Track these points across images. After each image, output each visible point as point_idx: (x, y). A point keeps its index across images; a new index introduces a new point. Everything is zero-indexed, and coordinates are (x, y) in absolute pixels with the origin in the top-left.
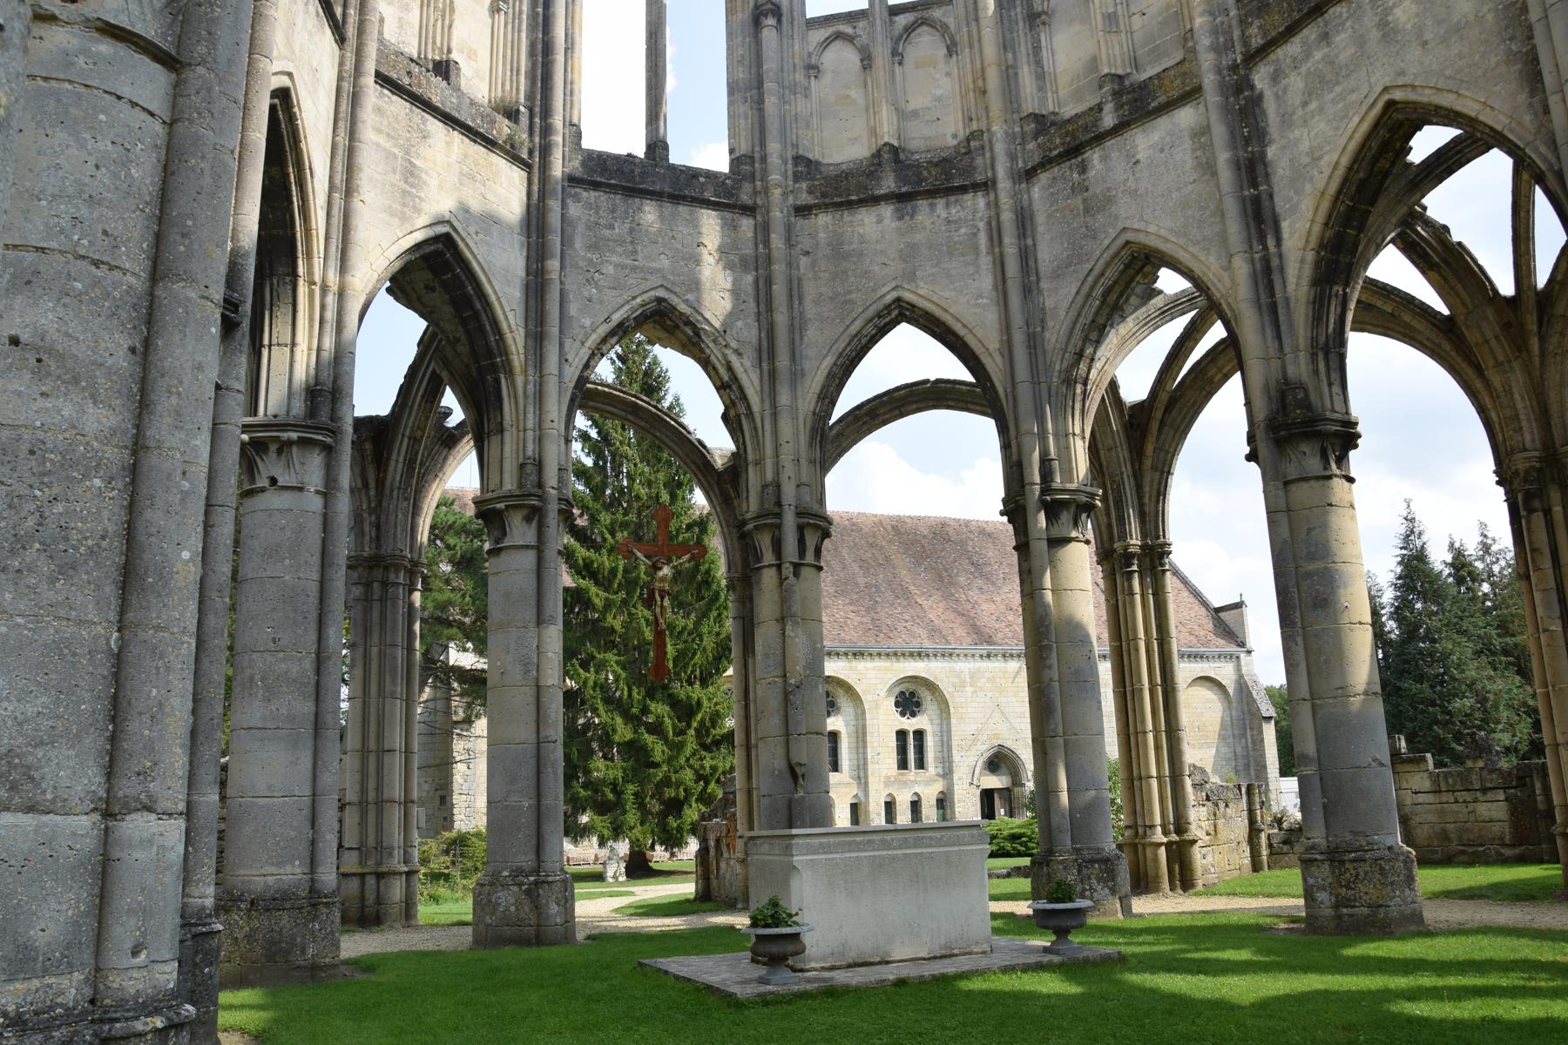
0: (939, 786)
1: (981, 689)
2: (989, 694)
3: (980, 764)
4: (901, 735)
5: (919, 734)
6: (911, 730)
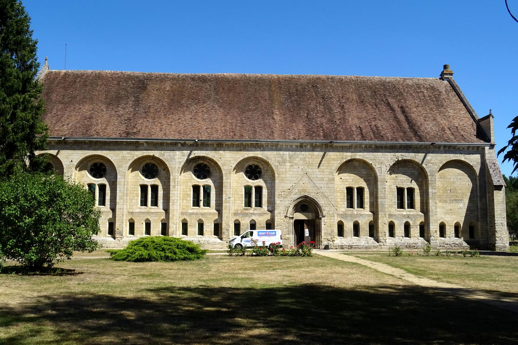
0: (268, 217)
1: (296, 164)
2: (301, 167)
3: (292, 206)
6: (97, 183)
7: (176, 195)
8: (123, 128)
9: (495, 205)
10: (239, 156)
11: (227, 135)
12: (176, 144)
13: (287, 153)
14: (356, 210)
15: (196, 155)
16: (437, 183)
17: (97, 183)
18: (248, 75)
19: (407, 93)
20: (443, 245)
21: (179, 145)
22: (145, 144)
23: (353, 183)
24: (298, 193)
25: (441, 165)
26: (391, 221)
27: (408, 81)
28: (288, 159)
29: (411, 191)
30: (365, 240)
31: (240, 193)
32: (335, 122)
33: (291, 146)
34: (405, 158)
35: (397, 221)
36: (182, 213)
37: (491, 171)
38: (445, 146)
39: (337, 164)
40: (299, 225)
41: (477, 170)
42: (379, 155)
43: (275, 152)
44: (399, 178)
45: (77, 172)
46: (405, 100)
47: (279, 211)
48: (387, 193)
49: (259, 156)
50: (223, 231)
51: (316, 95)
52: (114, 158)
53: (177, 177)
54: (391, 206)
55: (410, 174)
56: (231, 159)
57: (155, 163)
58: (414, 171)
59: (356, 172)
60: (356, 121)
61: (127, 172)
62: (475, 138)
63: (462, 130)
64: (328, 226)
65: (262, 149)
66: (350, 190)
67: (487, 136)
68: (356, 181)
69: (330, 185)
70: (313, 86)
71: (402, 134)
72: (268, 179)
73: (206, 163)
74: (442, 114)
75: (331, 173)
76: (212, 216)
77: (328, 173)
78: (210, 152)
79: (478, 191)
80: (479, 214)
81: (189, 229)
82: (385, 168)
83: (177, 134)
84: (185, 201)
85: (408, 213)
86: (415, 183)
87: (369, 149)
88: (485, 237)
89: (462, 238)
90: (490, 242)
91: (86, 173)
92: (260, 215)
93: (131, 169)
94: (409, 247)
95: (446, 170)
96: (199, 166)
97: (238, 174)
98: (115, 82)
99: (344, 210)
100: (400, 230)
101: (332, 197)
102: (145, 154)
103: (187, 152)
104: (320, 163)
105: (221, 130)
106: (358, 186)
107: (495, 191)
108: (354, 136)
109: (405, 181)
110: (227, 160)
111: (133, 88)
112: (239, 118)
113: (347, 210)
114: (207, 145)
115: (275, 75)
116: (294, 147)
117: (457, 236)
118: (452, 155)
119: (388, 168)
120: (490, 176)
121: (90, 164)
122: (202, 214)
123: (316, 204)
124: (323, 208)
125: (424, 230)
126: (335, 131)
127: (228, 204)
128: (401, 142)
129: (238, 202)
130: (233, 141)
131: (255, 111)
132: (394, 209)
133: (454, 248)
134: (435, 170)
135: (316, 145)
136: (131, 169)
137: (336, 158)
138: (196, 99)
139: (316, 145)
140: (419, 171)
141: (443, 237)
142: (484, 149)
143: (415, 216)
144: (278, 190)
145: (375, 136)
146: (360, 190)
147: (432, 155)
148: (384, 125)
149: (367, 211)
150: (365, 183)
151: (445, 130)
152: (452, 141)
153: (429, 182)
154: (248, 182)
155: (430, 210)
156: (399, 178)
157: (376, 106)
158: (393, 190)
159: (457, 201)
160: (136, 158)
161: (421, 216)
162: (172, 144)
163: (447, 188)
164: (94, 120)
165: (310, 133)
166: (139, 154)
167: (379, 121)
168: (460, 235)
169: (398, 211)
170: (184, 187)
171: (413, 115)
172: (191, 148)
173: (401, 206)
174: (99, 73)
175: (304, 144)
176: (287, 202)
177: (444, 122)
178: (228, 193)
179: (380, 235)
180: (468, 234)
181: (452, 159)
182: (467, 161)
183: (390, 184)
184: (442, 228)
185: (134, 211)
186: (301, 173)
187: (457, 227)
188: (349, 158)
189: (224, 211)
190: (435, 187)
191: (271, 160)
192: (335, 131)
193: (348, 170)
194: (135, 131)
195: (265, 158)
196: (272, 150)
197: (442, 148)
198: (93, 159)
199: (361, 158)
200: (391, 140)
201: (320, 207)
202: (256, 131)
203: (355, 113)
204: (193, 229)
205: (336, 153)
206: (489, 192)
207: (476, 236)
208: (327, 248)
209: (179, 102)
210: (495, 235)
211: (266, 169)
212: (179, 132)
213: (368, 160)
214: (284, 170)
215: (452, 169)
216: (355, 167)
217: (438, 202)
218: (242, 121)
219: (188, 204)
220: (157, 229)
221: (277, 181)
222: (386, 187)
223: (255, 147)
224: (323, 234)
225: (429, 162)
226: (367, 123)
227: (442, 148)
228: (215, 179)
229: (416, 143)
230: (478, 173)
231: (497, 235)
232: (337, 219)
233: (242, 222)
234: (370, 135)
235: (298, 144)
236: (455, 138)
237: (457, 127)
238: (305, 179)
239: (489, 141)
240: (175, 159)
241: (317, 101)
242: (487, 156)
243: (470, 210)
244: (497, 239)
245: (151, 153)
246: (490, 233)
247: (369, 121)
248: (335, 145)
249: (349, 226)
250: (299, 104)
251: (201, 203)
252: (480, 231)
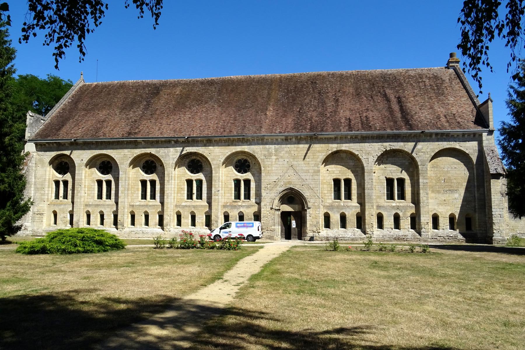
0: (255, 209)
1: (282, 157)
2: (286, 160)
3: (278, 198)
4: (237, 183)
5: (200, 182)
7: (170, 189)
8: (127, 129)
9: (492, 195)
10: (227, 151)
11: (217, 131)
12: (170, 142)
13: (273, 147)
14: (343, 201)
15: (188, 151)
16: (428, 172)
17: (104, 179)
18: (252, 76)
19: (407, 83)
20: (435, 237)
21: (173, 142)
22: (143, 142)
23: (339, 174)
24: (284, 186)
25: (433, 154)
26: (380, 213)
27: (410, 72)
28: (274, 152)
29: (401, 181)
30: (352, 231)
31: (229, 186)
32: (326, 115)
33: (277, 140)
34: (394, 148)
35: (386, 213)
36: (176, 206)
37: (488, 159)
38: (437, 134)
39: (322, 156)
40: (285, 217)
41: (474, 159)
42: (366, 146)
43: (261, 146)
44: (388, 169)
45: (87, 169)
46: (404, 90)
47: (265, 203)
48: (374, 184)
49: (246, 150)
50: (213, 222)
51: (313, 91)
52: (117, 156)
53: (170, 172)
54: (379, 197)
55: (400, 164)
56: (221, 154)
57: (153, 159)
58: (404, 161)
59: (343, 164)
60: (348, 114)
61: (128, 168)
62: (472, 125)
63: (459, 117)
64: (314, 217)
65: (249, 143)
66: (337, 182)
67: (486, 122)
68: (342, 172)
69: (316, 177)
70: (312, 82)
71: (392, 123)
72: (255, 172)
73: (199, 159)
74: (440, 102)
75: (317, 165)
76: (203, 208)
77: (313, 165)
78: (200, 148)
79: (476, 180)
80: (477, 205)
81: (183, 221)
82: (373, 159)
83: (172, 132)
84: (179, 195)
85: (398, 204)
86: (406, 174)
87: (355, 139)
88: (483, 229)
89: (458, 230)
90: (488, 235)
91: (95, 170)
92: (248, 207)
93: (132, 166)
94: (398, 239)
95: (439, 158)
96: (193, 161)
97: (227, 168)
98: (134, 90)
99: (330, 201)
100: (389, 222)
101: (318, 189)
102: (143, 152)
103: (179, 149)
104: (305, 156)
105: (213, 127)
106: (345, 177)
107: (492, 180)
108: (341, 128)
109: (395, 172)
110: (216, 155)
111: (147, 94)
112: (233, 116)
113: (334, 202)
114: (197, 141)
115: (278, 75)
116: (279, 140)
117: (452, 227)
118: (445, 143)
119: (375, 159)
120: (487, 163)
121: (99, 162)
122: (194, 207)
124: (308, 200)
125: (415, 222)
126: (323, 123)
127: (217, 197)
128: (389, 131)
129: (227, 195)
130: (221, 137)
131: (250, 109)
132: (384, 201)
133: (448, 240)
134: (426, 159)
135: (301, 137)
136: (132, 166)
137: (322, 150)
138: (200, 101)
139: (301, 137)
140: (410, 161)
141: (437, 229)
142: (481, 136)
143: (405, 207)
144: (264, 183)
145: (362, 127)
146: (348, 182)
147: (423, 143)
148: (376, 117)
149: (354, 202)
150: (352, 175)
151: (439, 118)
152: (446, 129)
153: (420, 172)
154: (237, 175)
155: (421, 201)
156: (388, 169)
157: (372, 97)
158: (382, 181)
159: (452, 191)
160: (135, 155)
161: (411, 207)
162: (165, 142)
163: (441, 178)
164: (105, 124)
165: (297, 127)
166: (138, 152)
167: (372, 112)
168: (455, 227)
169: (387, 202)
170: (179, 181)
171: (409, 105)
172: (184, 145)
173: (390, 197)
174: (123, 83)
175: (289, 137)
177: (440, 110)
178: (217, 186)
179: (367, 227)
180: (465, 226)
181: (445, 147)
182: (462, 149)
183: (377, 175)
184: (435, 220)
185: (134, 204)
186: (286, 165)
187: (452, 218)
188: (335, 150)
189: (213, 204)
190: (426, 177)
191: (257, 154)
192: (323, 123)
193: (335, 162)
194: (136, 131)
195: (251, 152)
196: (259, 144)
197: (434, 136)
198: (101, 158)
199: (347, 149)
200: (379, 130)
201: (305, 199)
202: (245, 126)
203: (348, 105)
204: (186, 221)
205: (321, 145)
206: (487, 182)
207: (473, 228)
208: (312, 239)
209: (183, 104)
210: (492, 227)
211: (254, 162)
212: (175, 131)
213: (354, 151)
214: (270, 163)
215: (444, 158)
216: (342, 159)
217: (430, 192)
218: (235, 117)
219: (182, 198)
220: (154, 221)
221: (263, 174)
222: (374, 178)
223: (242, 142)
224: (308, 225)
225: (420, 151)
226: (358, 115)
227: (434, 136)
228: (207, 173)
229: (406, 131)
230: (475, 161)
231: (494, 227)
232: (322, 212)
233: (231, 214)
234: (358, 126)
235: (283, 137)
236: (450, 125)
237: (454, 114)
238: (291, 172)
239: (488, 126)
240: (169, 156)
241: (312, 96)
242: (485, 143)
243: (466, 201)
244: (494, 231)
245: (148, 151)
246: (488, 225)
247: (361, 113)
248: (320, 137)
249: (335, 218)
250: (294, 100)
251: (194, 196)
252: (477, 223)
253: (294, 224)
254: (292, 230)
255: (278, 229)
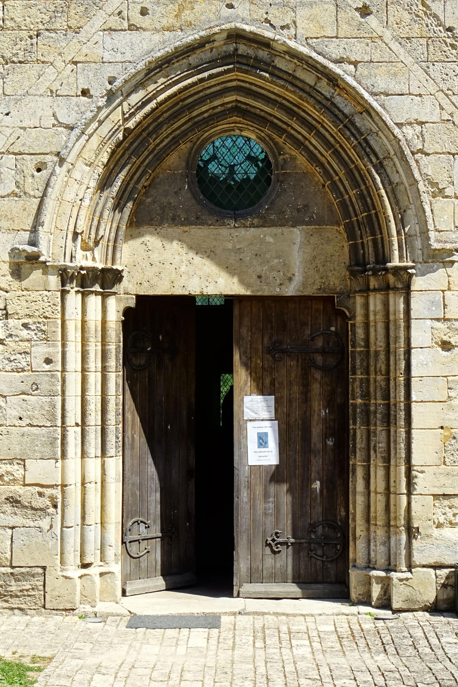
3: (90, 156)
40: (175, 361)
123: (346, 123)
124: (428, 168)
176: (41, 109)
224: (425, 447)
253: (258, 433)
254: (242, 497)
255: (100, 479)
